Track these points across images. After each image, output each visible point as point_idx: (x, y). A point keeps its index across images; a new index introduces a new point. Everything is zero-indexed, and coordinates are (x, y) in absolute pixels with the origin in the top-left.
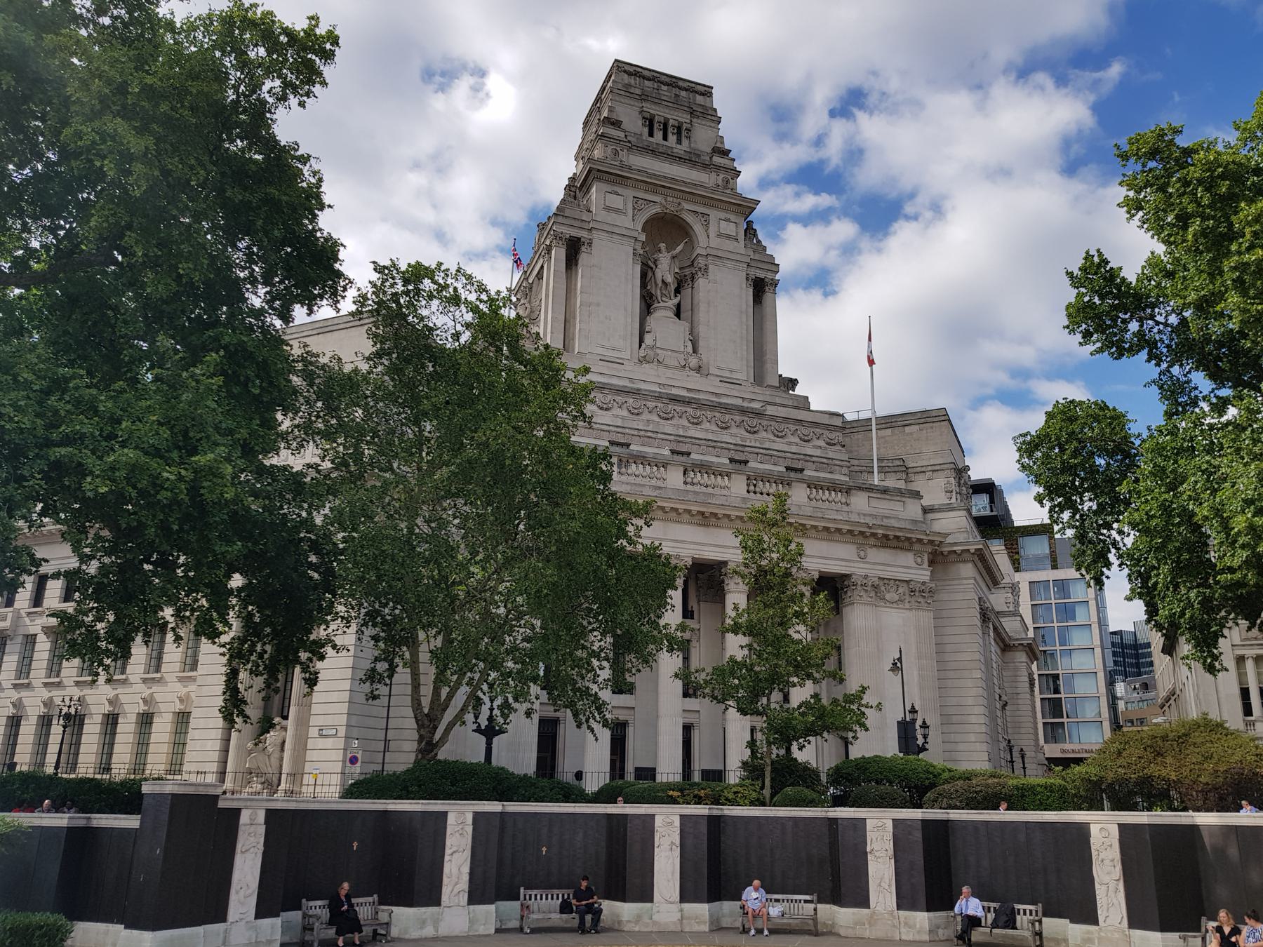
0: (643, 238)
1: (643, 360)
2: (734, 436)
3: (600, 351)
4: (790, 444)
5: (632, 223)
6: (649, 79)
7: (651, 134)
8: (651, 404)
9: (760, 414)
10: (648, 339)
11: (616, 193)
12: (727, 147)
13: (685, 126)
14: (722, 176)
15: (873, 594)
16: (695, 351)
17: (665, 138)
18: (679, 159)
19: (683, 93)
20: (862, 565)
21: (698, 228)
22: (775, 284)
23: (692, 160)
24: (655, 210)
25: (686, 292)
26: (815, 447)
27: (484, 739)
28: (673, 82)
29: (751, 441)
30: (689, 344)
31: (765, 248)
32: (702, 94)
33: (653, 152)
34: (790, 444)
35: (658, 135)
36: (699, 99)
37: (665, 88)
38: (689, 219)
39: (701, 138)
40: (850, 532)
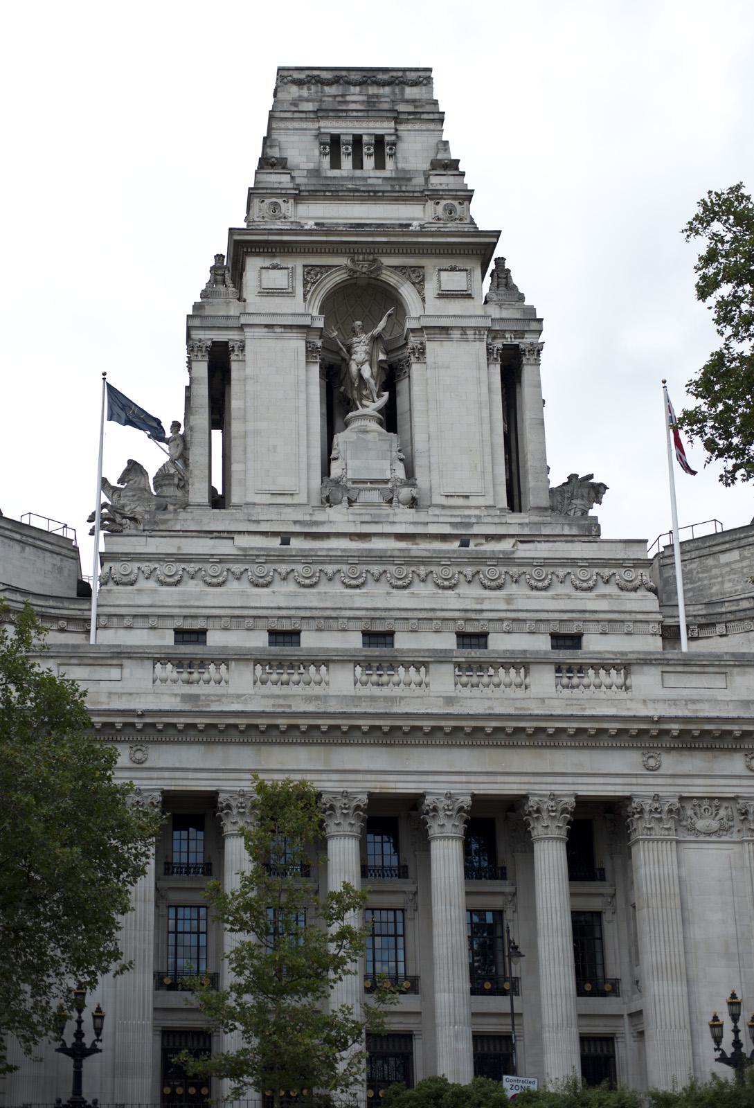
0: (320, 323)
1: (328, 501)
2: (466, 598)
5: (303, 307)
6: (330, 83)
7: (336, 164)
8: (330, 569)
9: (507, 560)
11: (275, 267)
12: (453, 157)
13: (387, 138)
14: (443, 203)
15: (670, 824)
16: (410, 473)
17: (358, 164)
18: (373, 196)
19: (387, 90)
20: (651, 781)
21: (407, 292)
22: (537, 350)
23: (400, 191)
25: (402, 386)
26: (604, 596)
28: (368, 77)
29: (494, 602)
30: (401, 465)
31: (521, 297)
32: (415, 84)
33: (334, 193)
35: (347, 163)
36: (411, 92)
37: (358, 88)
38: (391, 278)
39: (413, 151)
40: (621, 732)
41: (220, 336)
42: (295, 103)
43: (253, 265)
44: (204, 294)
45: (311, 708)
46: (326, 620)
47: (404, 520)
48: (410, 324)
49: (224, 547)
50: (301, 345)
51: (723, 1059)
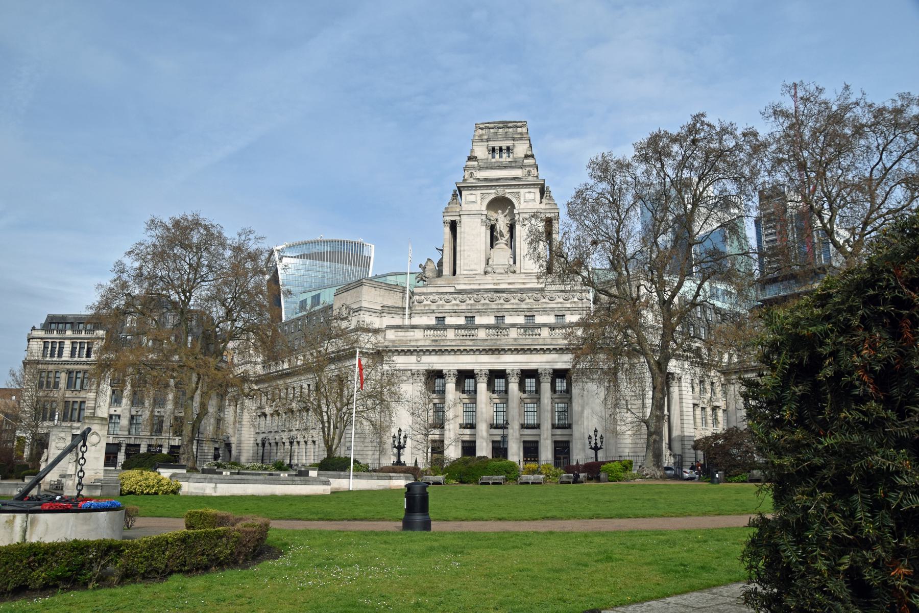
1: (486, 273)
3: (465, 272)
4: (557, 303)
7: (493, 157)
10: (490, 263)
16: (515, 263)
17: (501, 157)
19: (511, 130)
21: (514, 200)
24: (493, 196)
27: (395, 450)
34: (557, 303)
35: (497, 156)
36: (519, 130)
39: (521, 149)
41: (453, 218)
42: (481, 135)
43: (464, 193)
44: (449, 204)
45: (471, 343)
46: (484, 312)
47: (512, 278)
48: (516, 211)
49: (452, 290)
50: (480, 221)
51: (591, 448)
